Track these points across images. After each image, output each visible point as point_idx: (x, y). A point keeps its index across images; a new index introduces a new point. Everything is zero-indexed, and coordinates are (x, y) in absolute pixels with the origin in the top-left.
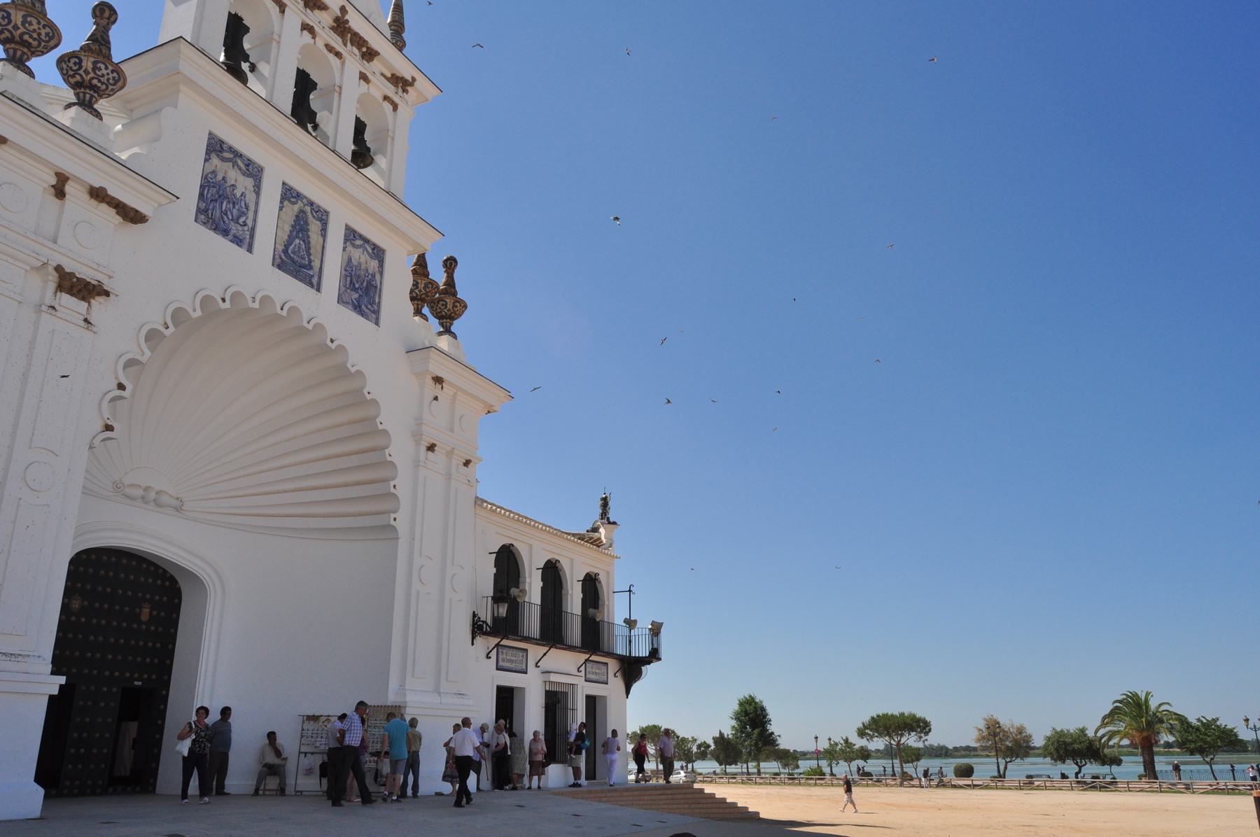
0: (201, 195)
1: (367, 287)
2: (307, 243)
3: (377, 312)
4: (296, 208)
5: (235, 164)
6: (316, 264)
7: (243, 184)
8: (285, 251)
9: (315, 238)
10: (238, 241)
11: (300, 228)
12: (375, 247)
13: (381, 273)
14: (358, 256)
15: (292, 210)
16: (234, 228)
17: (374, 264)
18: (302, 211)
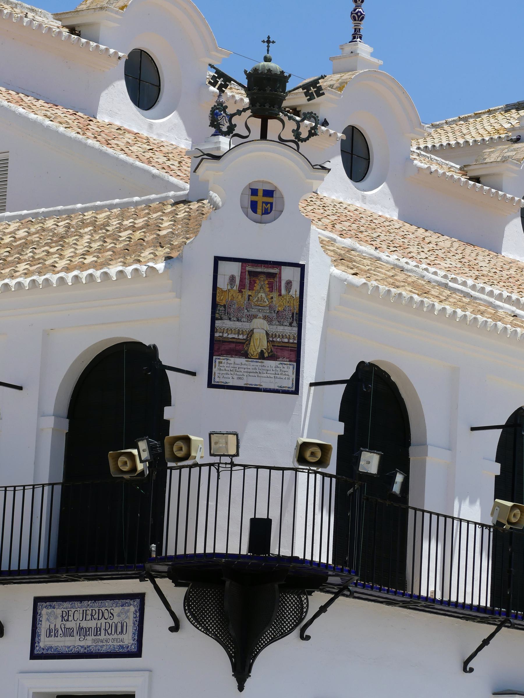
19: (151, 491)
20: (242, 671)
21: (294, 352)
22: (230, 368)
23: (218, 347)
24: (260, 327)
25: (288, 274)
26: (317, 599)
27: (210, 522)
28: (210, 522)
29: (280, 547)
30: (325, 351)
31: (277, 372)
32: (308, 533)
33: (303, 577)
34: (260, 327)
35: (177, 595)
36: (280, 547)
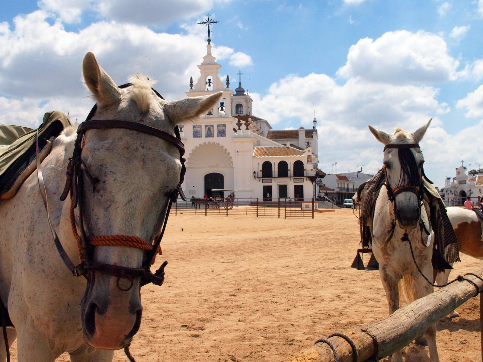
0: (193, 134)
1: (223, 132)
3: (225, 135)
4: (208, 127)
6: (212, 133)
7: (199, 129)
8: (207, 134)
10: (200, 137)
11: (209, 130)
12: (224, 125)
13: (225, 128)
14: (220, 128)
15: (207, 128)
16: (199, 136)
17: (224, 128)
18: (209, 127)
22: (309, 163)
23: (308, 161)
31: (310, 163)
35: (308, 178)
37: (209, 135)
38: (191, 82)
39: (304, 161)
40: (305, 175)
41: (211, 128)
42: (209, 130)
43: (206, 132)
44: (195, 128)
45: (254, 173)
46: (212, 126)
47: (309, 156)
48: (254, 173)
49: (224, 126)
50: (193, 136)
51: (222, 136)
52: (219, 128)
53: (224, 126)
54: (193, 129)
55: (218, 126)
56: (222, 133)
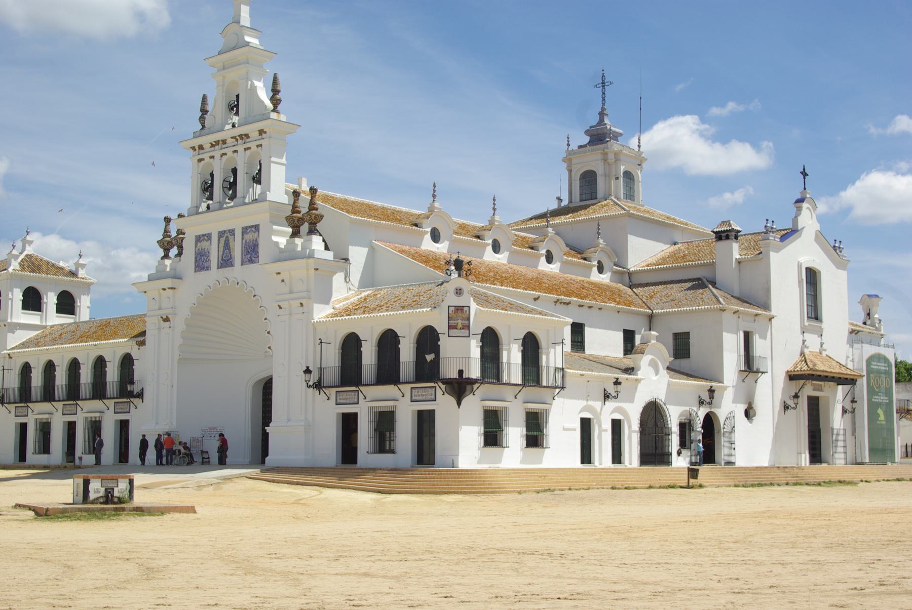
0: (196, 261)
2: (229, 249)
5: (204, 240)
9: (231, 244)
10: (208, 268)
14: (248, 237)
15: (223, 240)
16: (206, 264)
19: (436, 362)
20: (459, 404)
21: (468, 327)
22: (453, 332)
23: (450, 327)
24: (460, 322)
25: (466, 309)
26: (475, 386)
27: (449, 371)
28: (449, 371)
29: (465, 376)
30: (477, 327)
32: (475, 372)
33: (472, 382)
34: (460, 322)
35: (443, 387)
36: (465, 376)
37: (226, 262)
38: (204, 111)
39: (441, 326)
40: (442, 376)
41: (231, 238)
42: (227, 246)
43: (221, 253)
44: (199, 244)
45: (308, 371)
46: (232, 232)
47: (459, 309)
48: (308, 371)
49: (256, 228)
50: (196, 267)
51: (251, 261)
52: (245, 236)
53: (256, 228)
54: (196, 244)
55: (245, 230)
56: (251, 253)
